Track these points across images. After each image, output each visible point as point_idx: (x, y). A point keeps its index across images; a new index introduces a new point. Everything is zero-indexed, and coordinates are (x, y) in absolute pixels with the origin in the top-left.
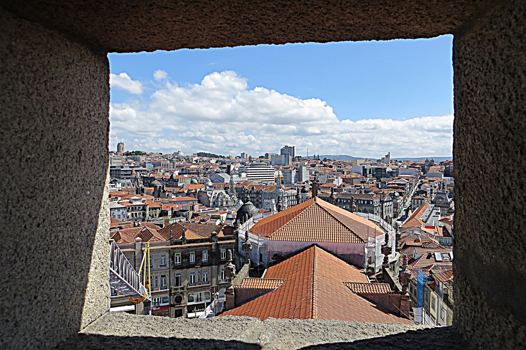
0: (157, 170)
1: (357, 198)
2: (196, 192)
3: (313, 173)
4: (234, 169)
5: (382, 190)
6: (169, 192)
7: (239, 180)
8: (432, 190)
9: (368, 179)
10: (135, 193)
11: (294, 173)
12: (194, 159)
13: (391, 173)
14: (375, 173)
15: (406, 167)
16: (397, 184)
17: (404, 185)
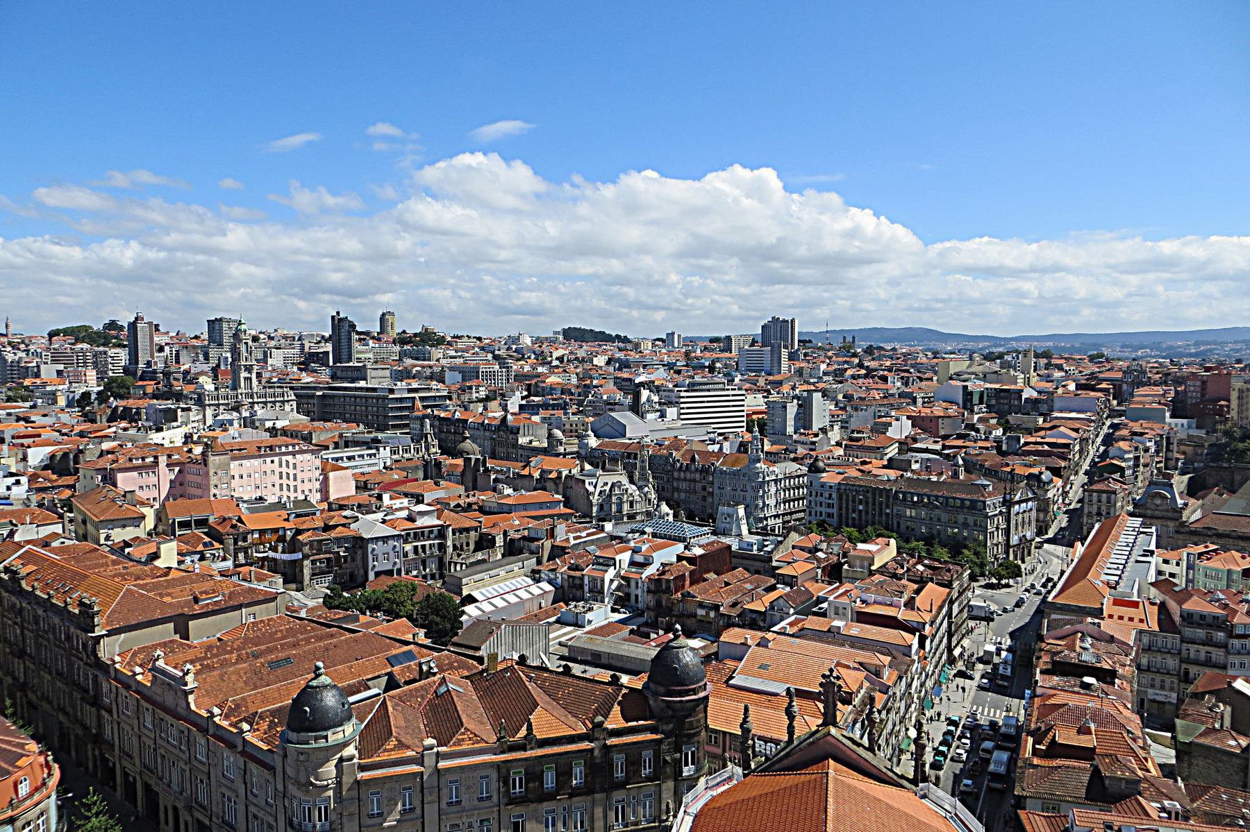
0: (470, 388)
1: (946, 494)
2: (559, 477)
3: (840, 397)
4: (648, 400)
5: (1009, 460)
6: (497, 472)
7: (660, 425)
8: (1137, 458)
9: (976, 417)
10: (421, 474)
11: (792, 409)
12: (556, 354)
13: (1034, 403)
14: (993, 402)
15: (1072, 387)
16: (1048, 444)
17: (1067, 446)
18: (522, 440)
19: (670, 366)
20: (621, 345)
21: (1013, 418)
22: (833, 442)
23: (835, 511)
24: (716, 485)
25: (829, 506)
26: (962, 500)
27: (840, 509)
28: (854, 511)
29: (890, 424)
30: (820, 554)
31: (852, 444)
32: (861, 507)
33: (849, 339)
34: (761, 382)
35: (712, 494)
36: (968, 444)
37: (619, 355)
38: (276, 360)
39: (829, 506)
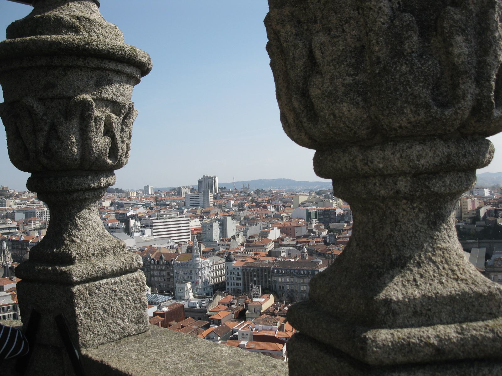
3: (242, 218)
4: (135, 225)
9: (313, 225)
14: (322, 217)
19: (146, 206)
20: (119, 194)
21: (332, 225)
22: (239, 244)
23: (241, 282)
24: (175, 272)
25: (238, 279)
26: (308, 271)
27: (244, 280)
28: (251, 281)
29: (269, 232)
30: (233, 306)
31: (249, 244)
32: (255, 279)
33: (246, 186)
34: (199, 212)
35: (173, 277)
36: (309, 240)
37: (118, 200)
39: (238, 279)
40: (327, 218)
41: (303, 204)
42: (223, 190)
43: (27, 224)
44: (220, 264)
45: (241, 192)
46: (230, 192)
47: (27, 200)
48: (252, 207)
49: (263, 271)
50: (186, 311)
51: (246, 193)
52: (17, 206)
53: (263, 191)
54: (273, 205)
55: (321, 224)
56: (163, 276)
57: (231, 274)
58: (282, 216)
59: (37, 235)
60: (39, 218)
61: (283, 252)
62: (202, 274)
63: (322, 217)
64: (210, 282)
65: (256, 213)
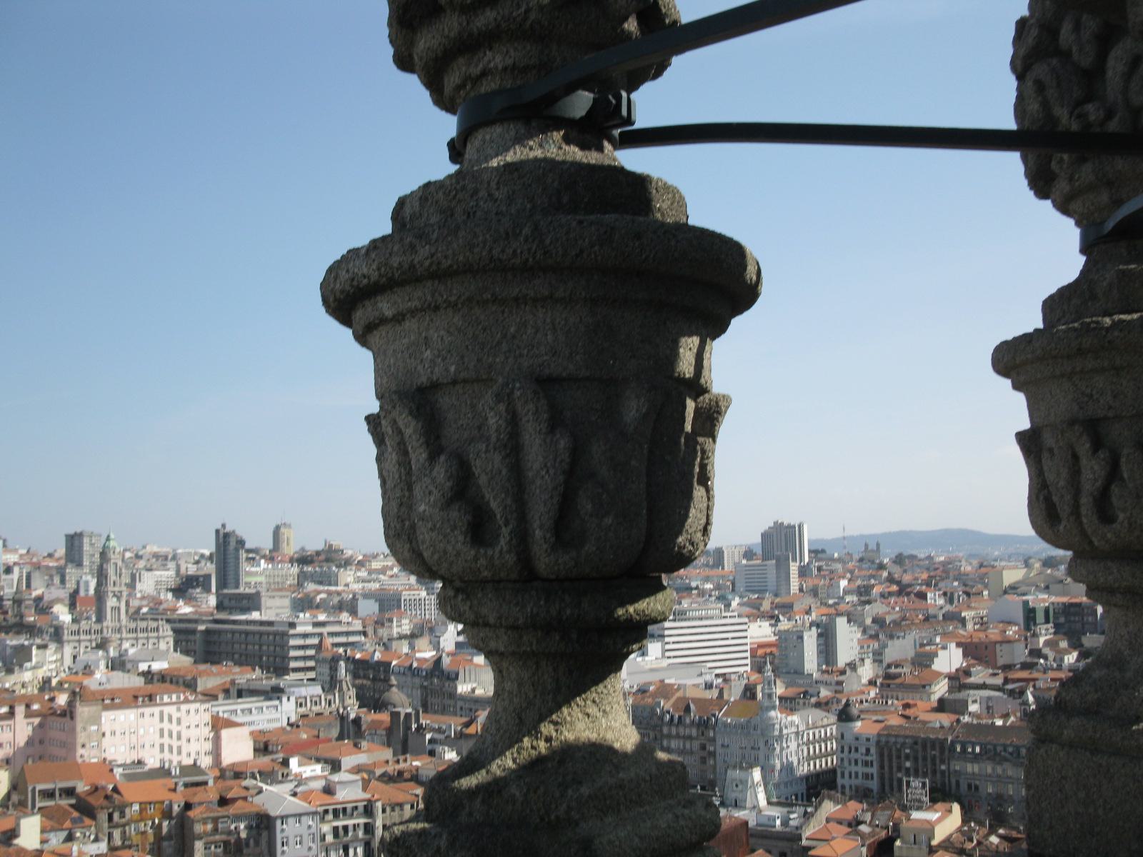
3: (868, 621)
9: (1042, 640)
14: (1062, 620)
18: (463, 688)
22: (865, 681)
23: (874, 770)
24: (719, 742)
25: (866, 764)
27: (882, 767)
28: (899, 769)
29: (936, 655)
30: (864, 828)
31: (889, 681)
32: (908, 764)
33: (872, 546)
34: (766, 606)
35: (713, 754)
36: (1035, 675)
38: (147, 584)
39: (866, 764)
40: (1074, 622)
41: (1013, 588)
42: (819, 555)
43: (383, 625)
44: (823, 727)
45: (861, 560)
46: (833, 560)
47: (383, 571)
48: (890, 594)
49: (929, 745)
50: (752, 835)
51: (873, 562)
52: (360, 585)
53: (913, 557)
54: (939, 590)
55: (1060, 636)
56: (692, 753)
57: (850, 752)
58: (964, 618)
59: (405, 649)
60: (409, 612)
61: (974, 702)
62: (782, 749)
63: (1062, 620)
64: (801, 768)
65: (901, 610)
